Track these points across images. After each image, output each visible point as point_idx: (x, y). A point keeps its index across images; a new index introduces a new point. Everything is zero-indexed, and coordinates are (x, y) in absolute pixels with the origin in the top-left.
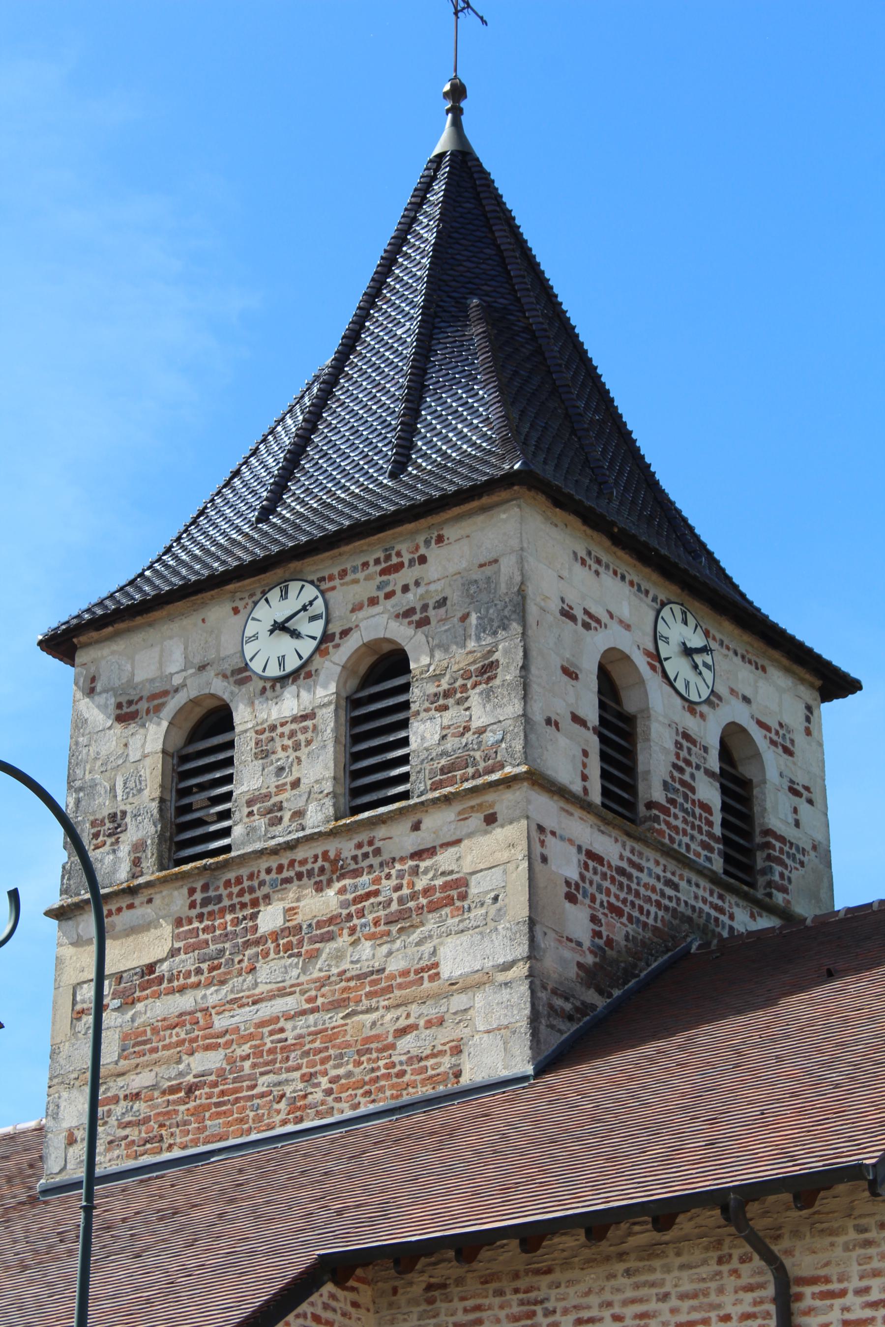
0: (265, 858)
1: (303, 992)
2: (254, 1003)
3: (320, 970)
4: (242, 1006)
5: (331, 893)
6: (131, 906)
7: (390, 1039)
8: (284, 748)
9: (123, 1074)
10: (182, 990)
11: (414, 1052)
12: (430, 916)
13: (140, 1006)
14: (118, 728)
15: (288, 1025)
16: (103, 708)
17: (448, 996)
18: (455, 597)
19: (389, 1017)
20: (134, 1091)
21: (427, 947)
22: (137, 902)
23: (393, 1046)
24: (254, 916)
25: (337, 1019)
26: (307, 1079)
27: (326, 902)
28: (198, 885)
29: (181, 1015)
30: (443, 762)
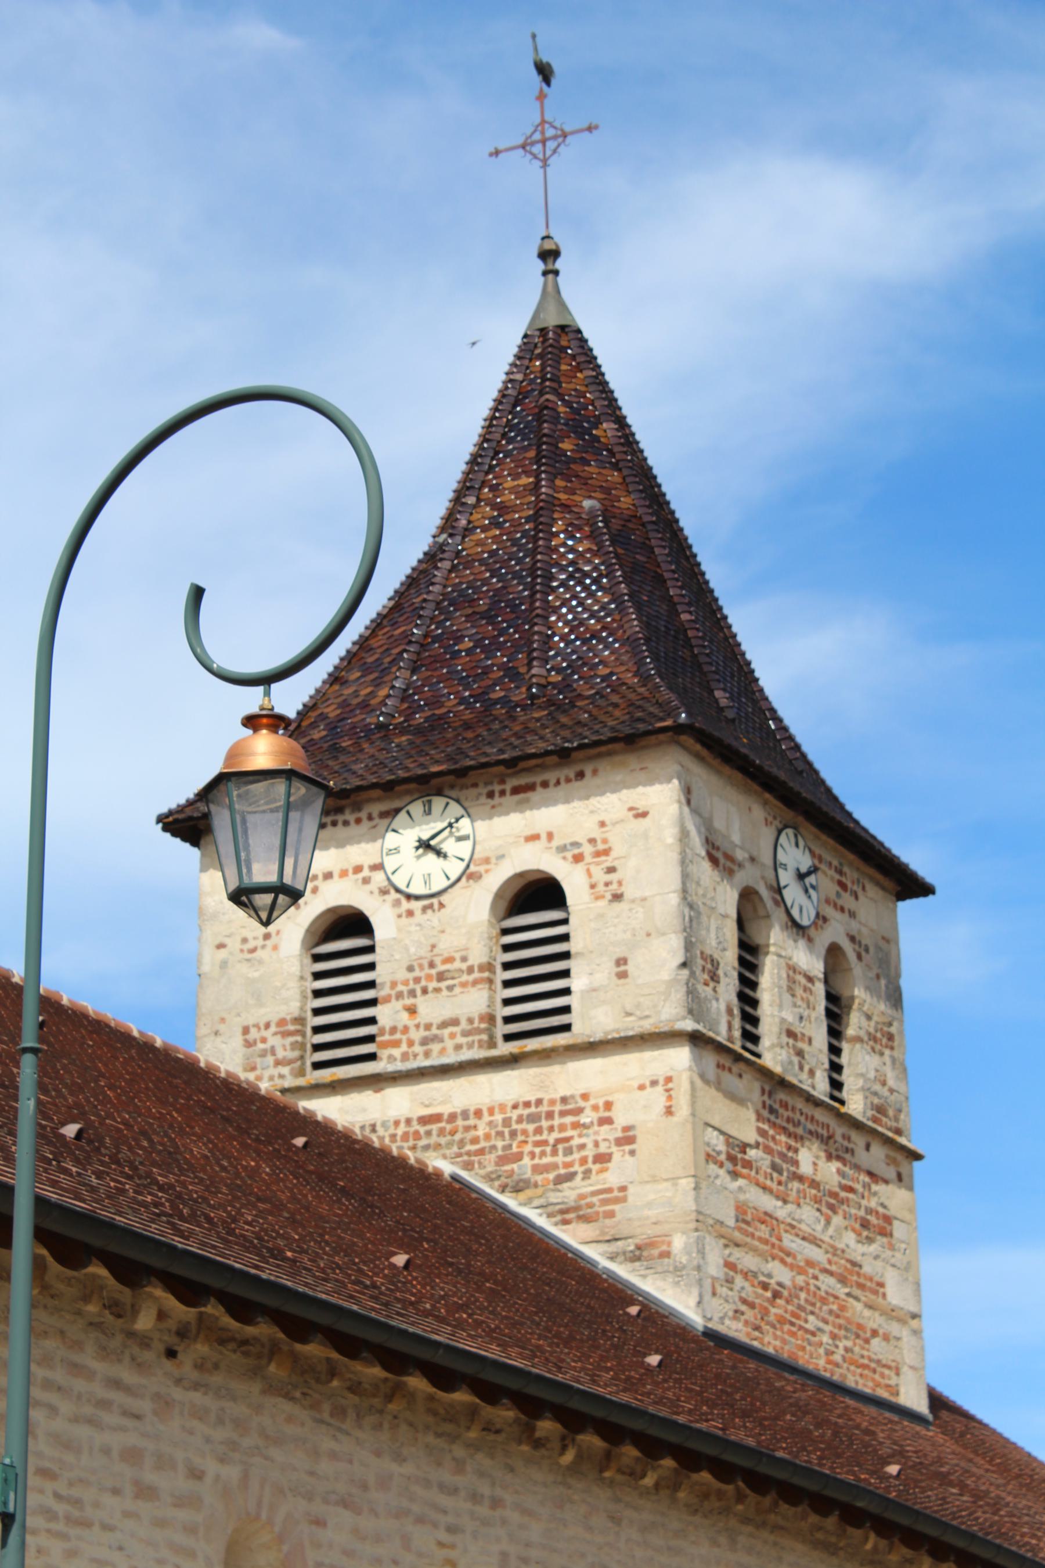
0: (801, 1099)
1: (827, 1252)
2: (804, 1239)
3: (831, 1237)
4: (797, 1235)
5: (834, 1166)
6: (730, 1070)
7: (868, 1335)
8: (802, 999)
9: (737, 1245)
10: (764, 1188)
11: (880, 1357)
12: (879, 1237)
13: (741, 1182)
14: (706, 865)
15: (821, 1277)
16: (699, 832)
17: (892, 1318)
18: (872, 949)
19: (867, 1313)
20: (745, 1270)
21: (879, 1264)
22: (735, 1069)
23: (867, 1341)
24: (796, 1151)
25: (842, 1291)
26: (834, 1337)
27: (830, 1172)
28: (767, 1088)
29: (766, 1213)
30: (876, 1101)
